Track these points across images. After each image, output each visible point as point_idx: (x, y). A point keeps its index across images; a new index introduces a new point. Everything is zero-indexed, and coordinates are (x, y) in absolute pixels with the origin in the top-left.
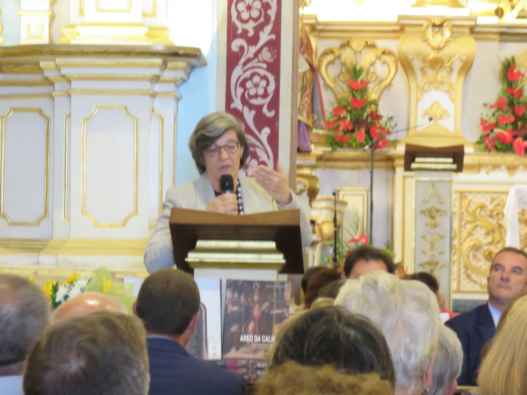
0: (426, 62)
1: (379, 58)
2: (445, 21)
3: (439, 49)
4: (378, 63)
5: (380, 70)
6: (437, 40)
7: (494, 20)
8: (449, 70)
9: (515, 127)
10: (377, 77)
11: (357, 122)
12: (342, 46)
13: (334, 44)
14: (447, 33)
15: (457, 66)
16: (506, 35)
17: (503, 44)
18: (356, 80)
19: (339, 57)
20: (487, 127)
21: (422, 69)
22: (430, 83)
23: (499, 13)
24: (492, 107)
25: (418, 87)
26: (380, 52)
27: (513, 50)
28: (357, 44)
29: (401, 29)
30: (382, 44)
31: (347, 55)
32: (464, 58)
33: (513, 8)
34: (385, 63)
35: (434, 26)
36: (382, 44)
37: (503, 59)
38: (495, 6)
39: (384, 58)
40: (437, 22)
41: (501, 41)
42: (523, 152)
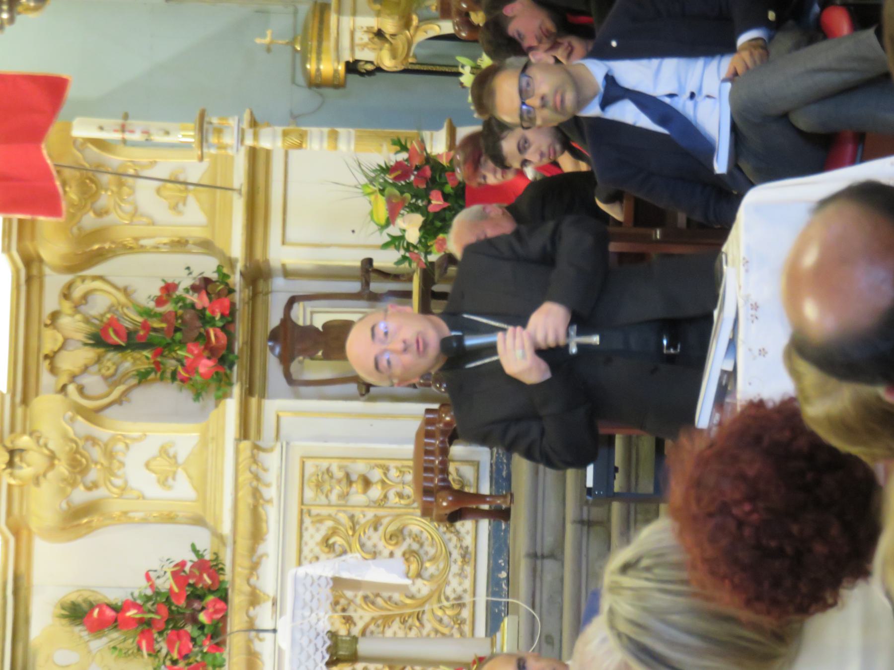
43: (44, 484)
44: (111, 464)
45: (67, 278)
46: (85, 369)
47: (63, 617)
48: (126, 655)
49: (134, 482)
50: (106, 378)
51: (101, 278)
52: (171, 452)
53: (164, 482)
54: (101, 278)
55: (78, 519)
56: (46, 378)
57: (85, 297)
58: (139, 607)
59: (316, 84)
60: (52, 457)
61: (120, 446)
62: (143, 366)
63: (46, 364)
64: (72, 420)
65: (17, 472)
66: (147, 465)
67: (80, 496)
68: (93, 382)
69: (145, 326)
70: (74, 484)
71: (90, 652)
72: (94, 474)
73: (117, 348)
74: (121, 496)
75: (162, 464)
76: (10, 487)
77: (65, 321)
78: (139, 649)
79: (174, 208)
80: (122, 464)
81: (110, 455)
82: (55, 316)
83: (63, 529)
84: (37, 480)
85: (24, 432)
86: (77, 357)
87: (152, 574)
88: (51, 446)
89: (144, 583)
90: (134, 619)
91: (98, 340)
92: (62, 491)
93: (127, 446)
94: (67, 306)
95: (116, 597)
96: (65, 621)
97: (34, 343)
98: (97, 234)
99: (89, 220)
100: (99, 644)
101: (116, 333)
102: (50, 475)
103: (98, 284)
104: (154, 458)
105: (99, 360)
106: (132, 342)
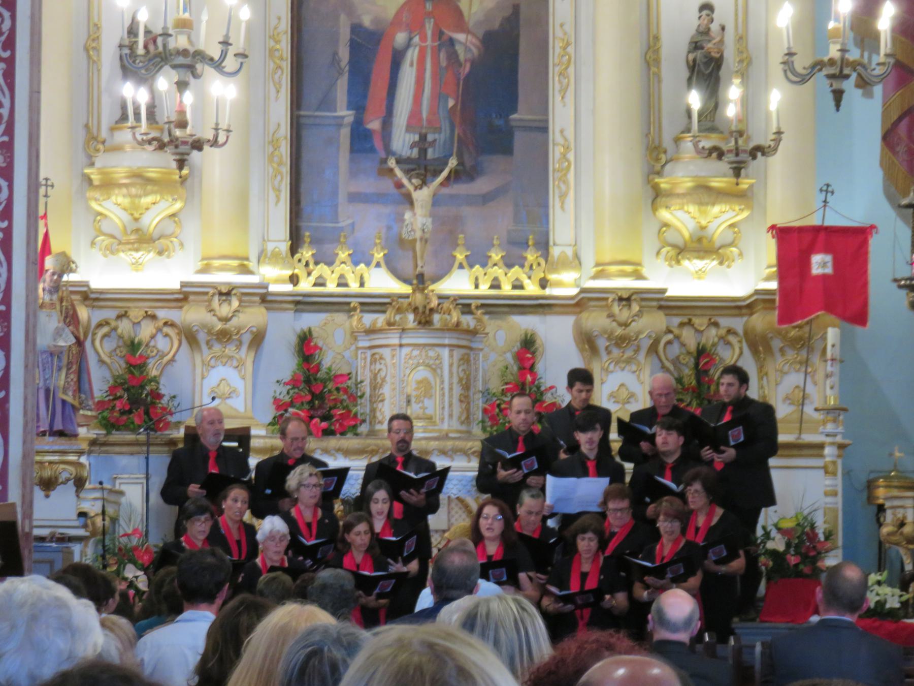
0: (212, 334)
1: (159, 330)
2: (233, 289)
3: (226, 320)
4: (159, 337)
5: (161, 343)
6: (224, 310)
7: (289, 288)
8: (238, 343)
9: (312, 407)
10: (158, 351)
11: (135, 402)
12: (119, 317)
13: (110, 314)
14: (235, 303)
15: (247, 338)
16: (302, 303)
17: (297, 314)
18: (134, 355)
19: (115, 329)
20: (280, 405)
21: (208, 343)
22: (217, 358)
23: (294, 279)
24: (286, 384)
25: (203, 363)
26: (161, 323)
27: (310, 320)
28: (136, 313)
29: (183, 296)
30: (163, 314)
31: (124, 327)
32: (254, 330)
33: (309, 274)
34: (167, 335)
35: (221, 294)
36: (163, 314)
37: (298, 330)
38: (289, 272)
39: (166, 330)
40: (224, 290)
41: (296, 311)
42: (320, 433)
43: (608, 321)
44: (624, 362)
45: (740, 331)
46: (683, 345)
47: (526, 335)
48: (503, 376)
49: (611, 376)
50: (678, 358)
51: (741, 353)
52: (632, 400)
53: (612, 395)
54: (741, 353)
55: (587, 342)
56: (676, 321)
57: (728, 343)
58: (533, 382)
59: (870, 486)
60: (626, 325)
61: (634, 368)
62: (686, 381)
63: (685, 320)
64: (649, 337)
65: (616, 304)
66: (622, 385)
67: (602, 343)
68: (675, 350)
69: (711, 381)
70: (609, 339)
71: (505, 353)
72: (616, 352)
73: (697, 364)
74: (602, 369)
75: (624, 394)
76: (607, 299)
77: (713, 331)
78: (507, 384)
79: (787, 398)
80: (623, 369)
81: (629, 361)
82: (716, 325)
83: (581, 333)
84: (611, 316)
85: (641, 307)
86: (689, 338)
87: (554, 390)
88: (633, 324)
89: (548, 385)
90: (525, 379)
91: (701, 352)
92: (605, 332)
93: (634, 372)
94: (722, 332)
95: (539, 367)
96: (523, 336)
97: (698, 312)
98: (769, 350)
99: (777, 344)
100: (509, 357)
101: (706, 364)
102: (615, 324)
103: (737, 351)
104: (627, 389)
105: (689, 353)
106: (701, 373)
